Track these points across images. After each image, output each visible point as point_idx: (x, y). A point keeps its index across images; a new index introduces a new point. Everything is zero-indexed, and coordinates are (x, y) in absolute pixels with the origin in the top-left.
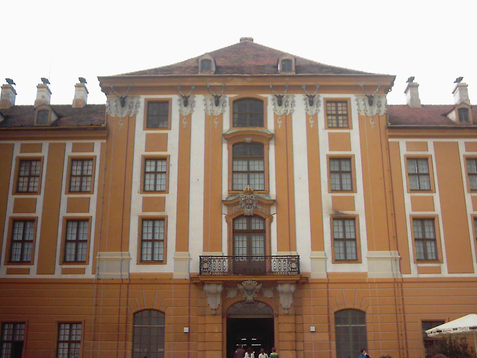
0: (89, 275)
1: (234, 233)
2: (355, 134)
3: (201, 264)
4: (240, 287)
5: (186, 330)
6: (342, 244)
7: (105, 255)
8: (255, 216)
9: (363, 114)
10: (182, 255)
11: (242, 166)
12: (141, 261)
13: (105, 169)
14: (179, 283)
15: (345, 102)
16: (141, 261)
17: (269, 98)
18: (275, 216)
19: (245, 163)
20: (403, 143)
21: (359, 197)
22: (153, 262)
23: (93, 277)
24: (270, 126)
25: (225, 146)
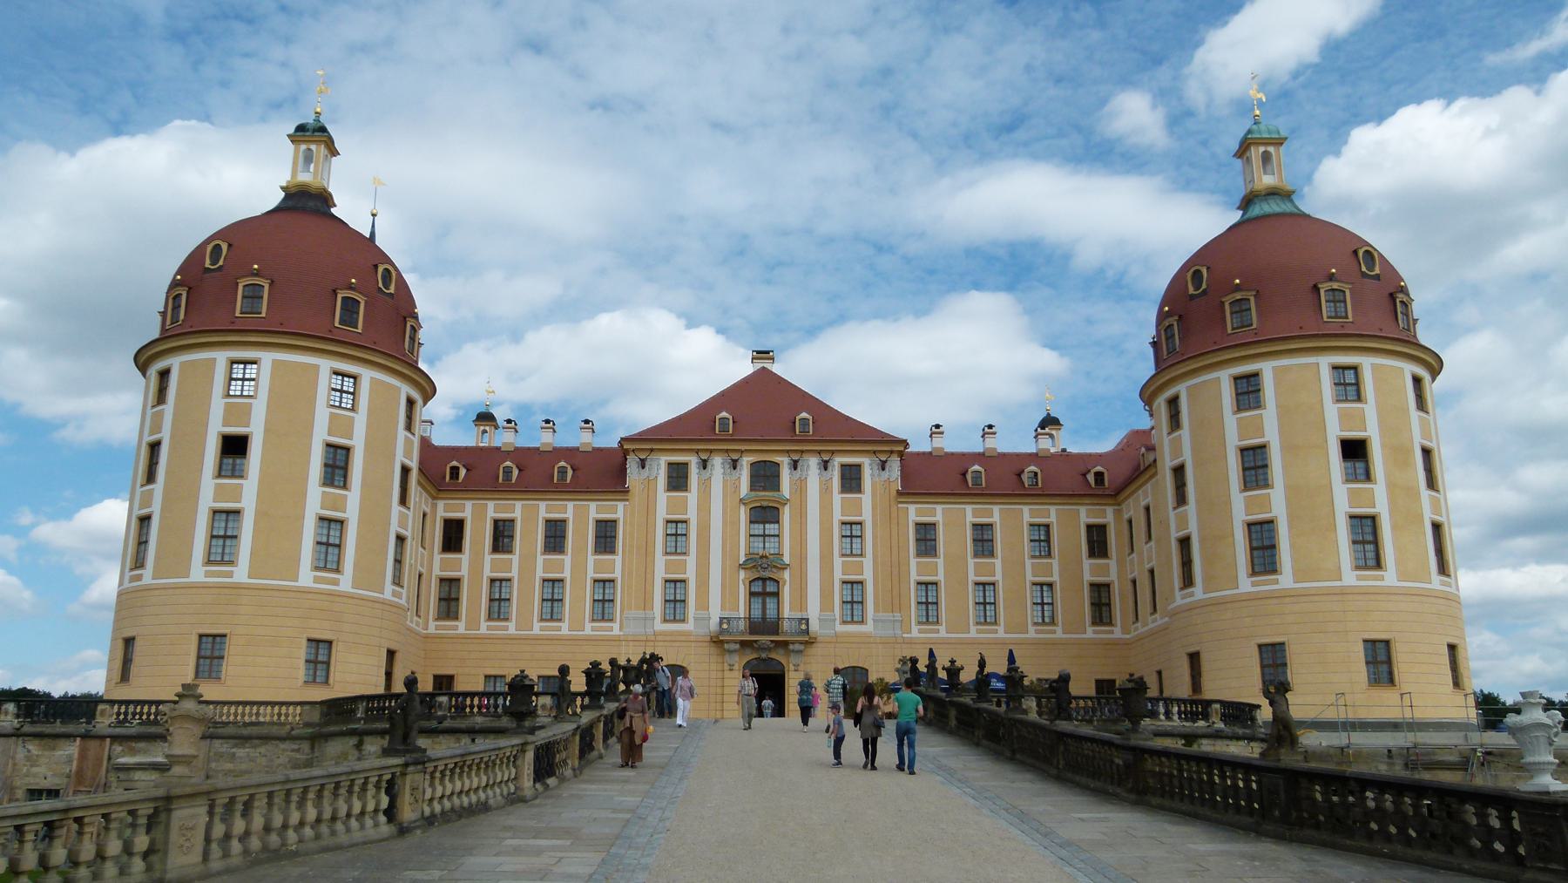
3: (721, 623)
4: (755, 645)
6: (849, 606)
8: (771, 579)
10: (702, 613)
11: (758, 529)
15: (858, 467)
17: (784, 461)
18: (788, 583)
19: (761, 526)
20: (912, 508)
21: (868, 562)
22: (675, 620)
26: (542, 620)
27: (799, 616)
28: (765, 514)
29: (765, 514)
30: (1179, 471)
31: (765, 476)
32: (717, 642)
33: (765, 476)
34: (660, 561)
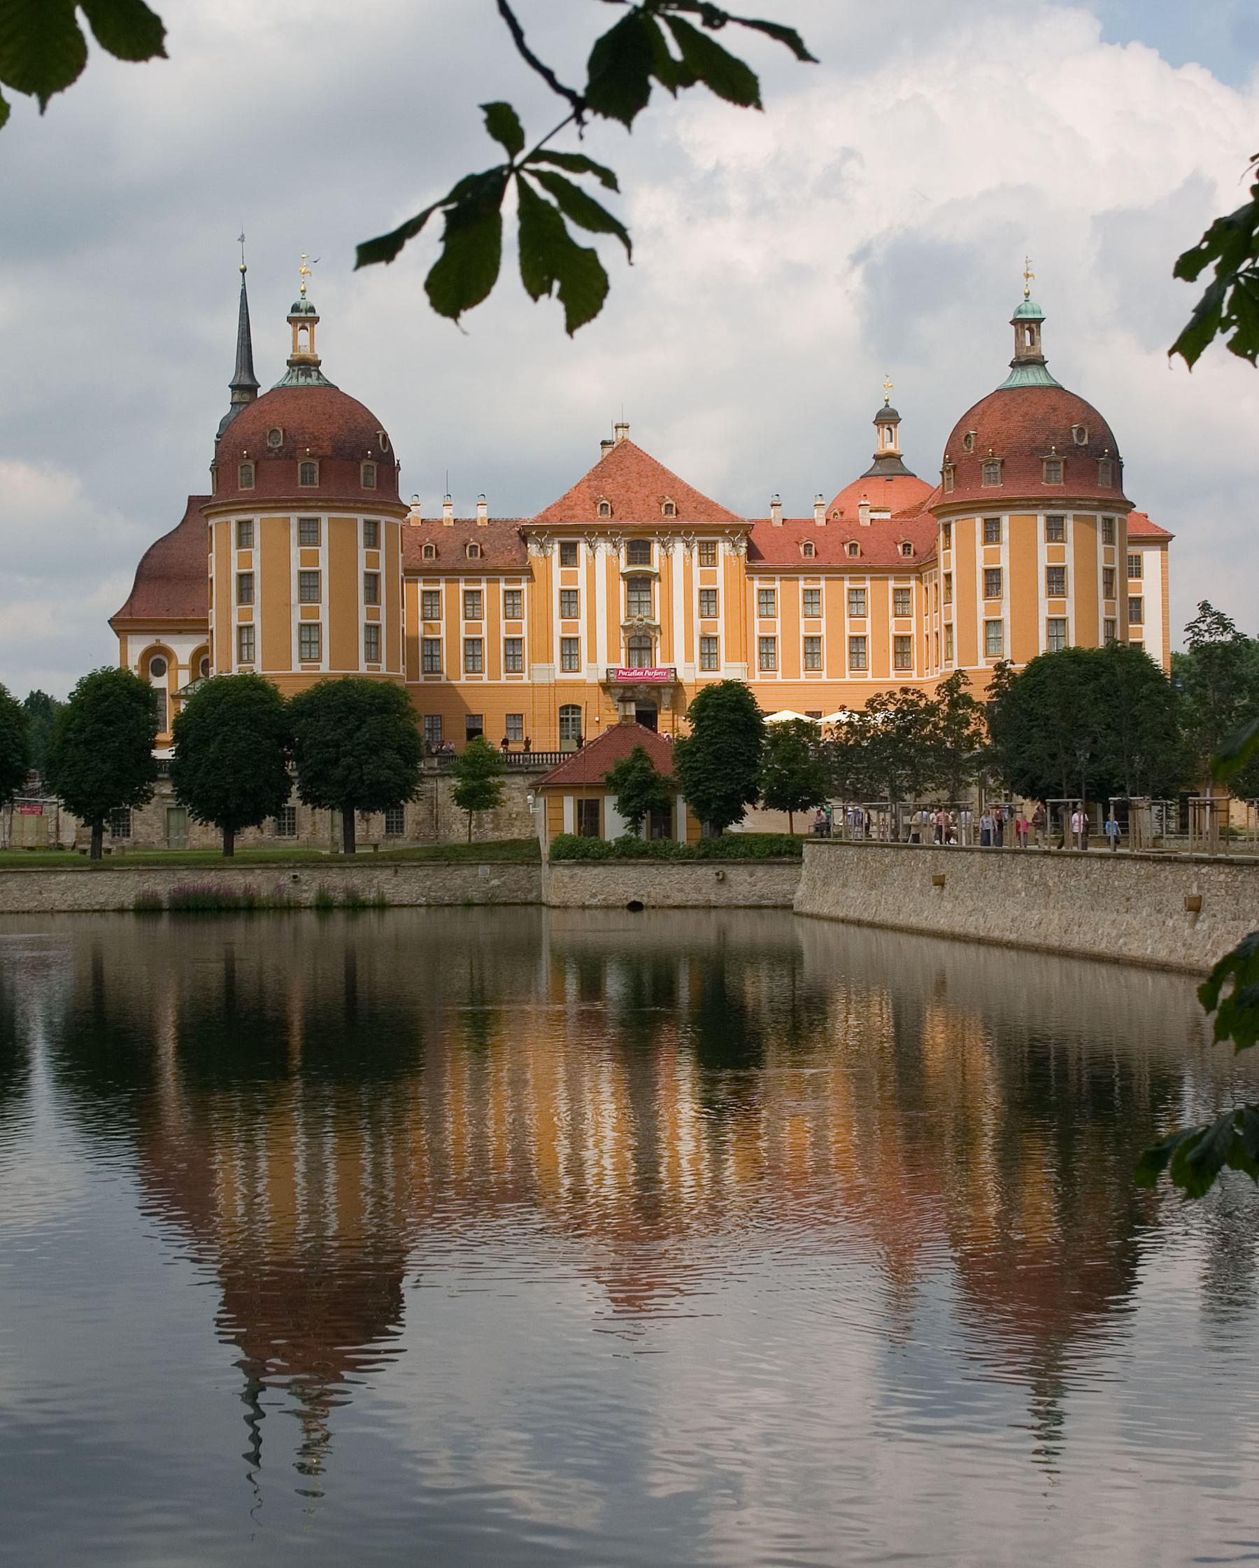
0: (526, 680)
1: (630, 649)
2: (720, 570)
5: (597, 719)
7: (536, 666)
9: (727, 554)
10: (592, 665)
12: (563, 671)
13: (532, 600)
14: (592, 686)
16: (563, 671)
21: (721, 622)
22: (571, 670)
23: (529, 682)
24: (655, 567)
25: (622, 583)
26: (467, 672)
27: (667, 666)
28: (639, 583)
29: (639, 583)
30: (948, 577)
31: (639, 551)
32: (606, 687)
33: (639, 551)
34: (557, 623)
